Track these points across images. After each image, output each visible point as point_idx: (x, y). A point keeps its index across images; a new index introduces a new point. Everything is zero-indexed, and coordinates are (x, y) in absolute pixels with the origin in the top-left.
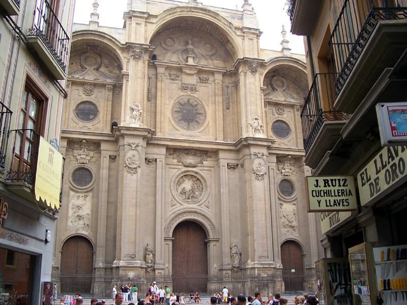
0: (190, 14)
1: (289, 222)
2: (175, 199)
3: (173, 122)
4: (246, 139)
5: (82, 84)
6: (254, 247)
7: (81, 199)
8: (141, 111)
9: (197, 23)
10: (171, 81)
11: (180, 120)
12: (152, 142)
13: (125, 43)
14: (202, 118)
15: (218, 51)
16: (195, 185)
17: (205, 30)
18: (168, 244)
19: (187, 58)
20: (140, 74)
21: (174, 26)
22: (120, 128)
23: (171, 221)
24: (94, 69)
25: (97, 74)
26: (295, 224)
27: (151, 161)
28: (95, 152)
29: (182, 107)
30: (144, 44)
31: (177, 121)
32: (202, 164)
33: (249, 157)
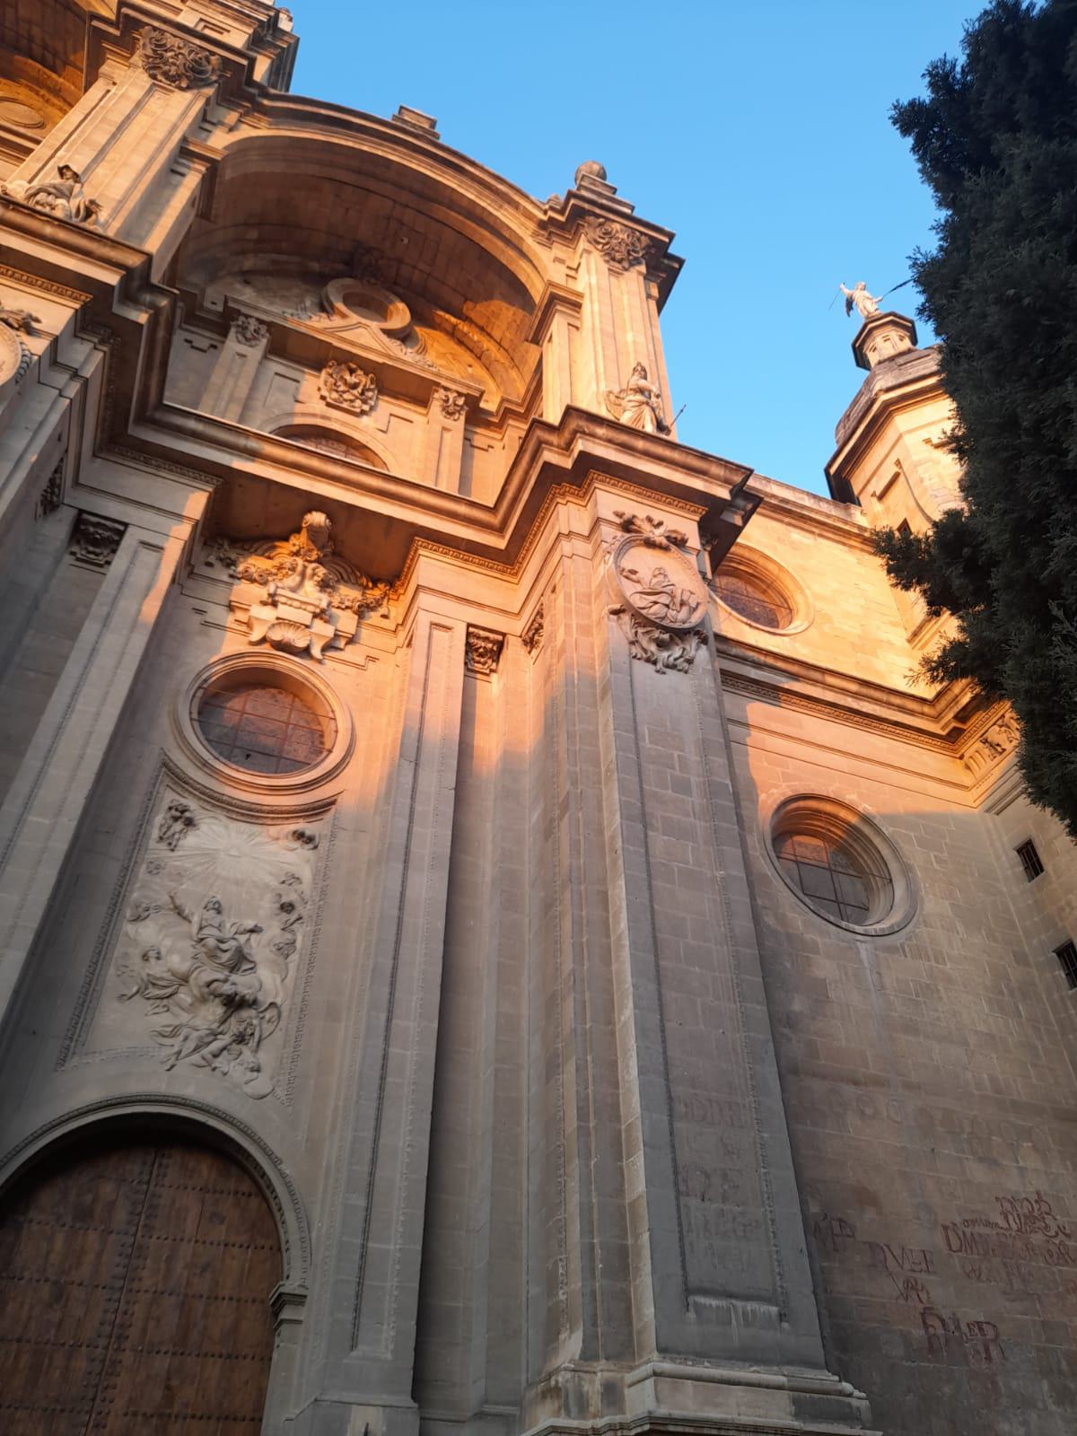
1: (212, 955)
26: (266, 980)
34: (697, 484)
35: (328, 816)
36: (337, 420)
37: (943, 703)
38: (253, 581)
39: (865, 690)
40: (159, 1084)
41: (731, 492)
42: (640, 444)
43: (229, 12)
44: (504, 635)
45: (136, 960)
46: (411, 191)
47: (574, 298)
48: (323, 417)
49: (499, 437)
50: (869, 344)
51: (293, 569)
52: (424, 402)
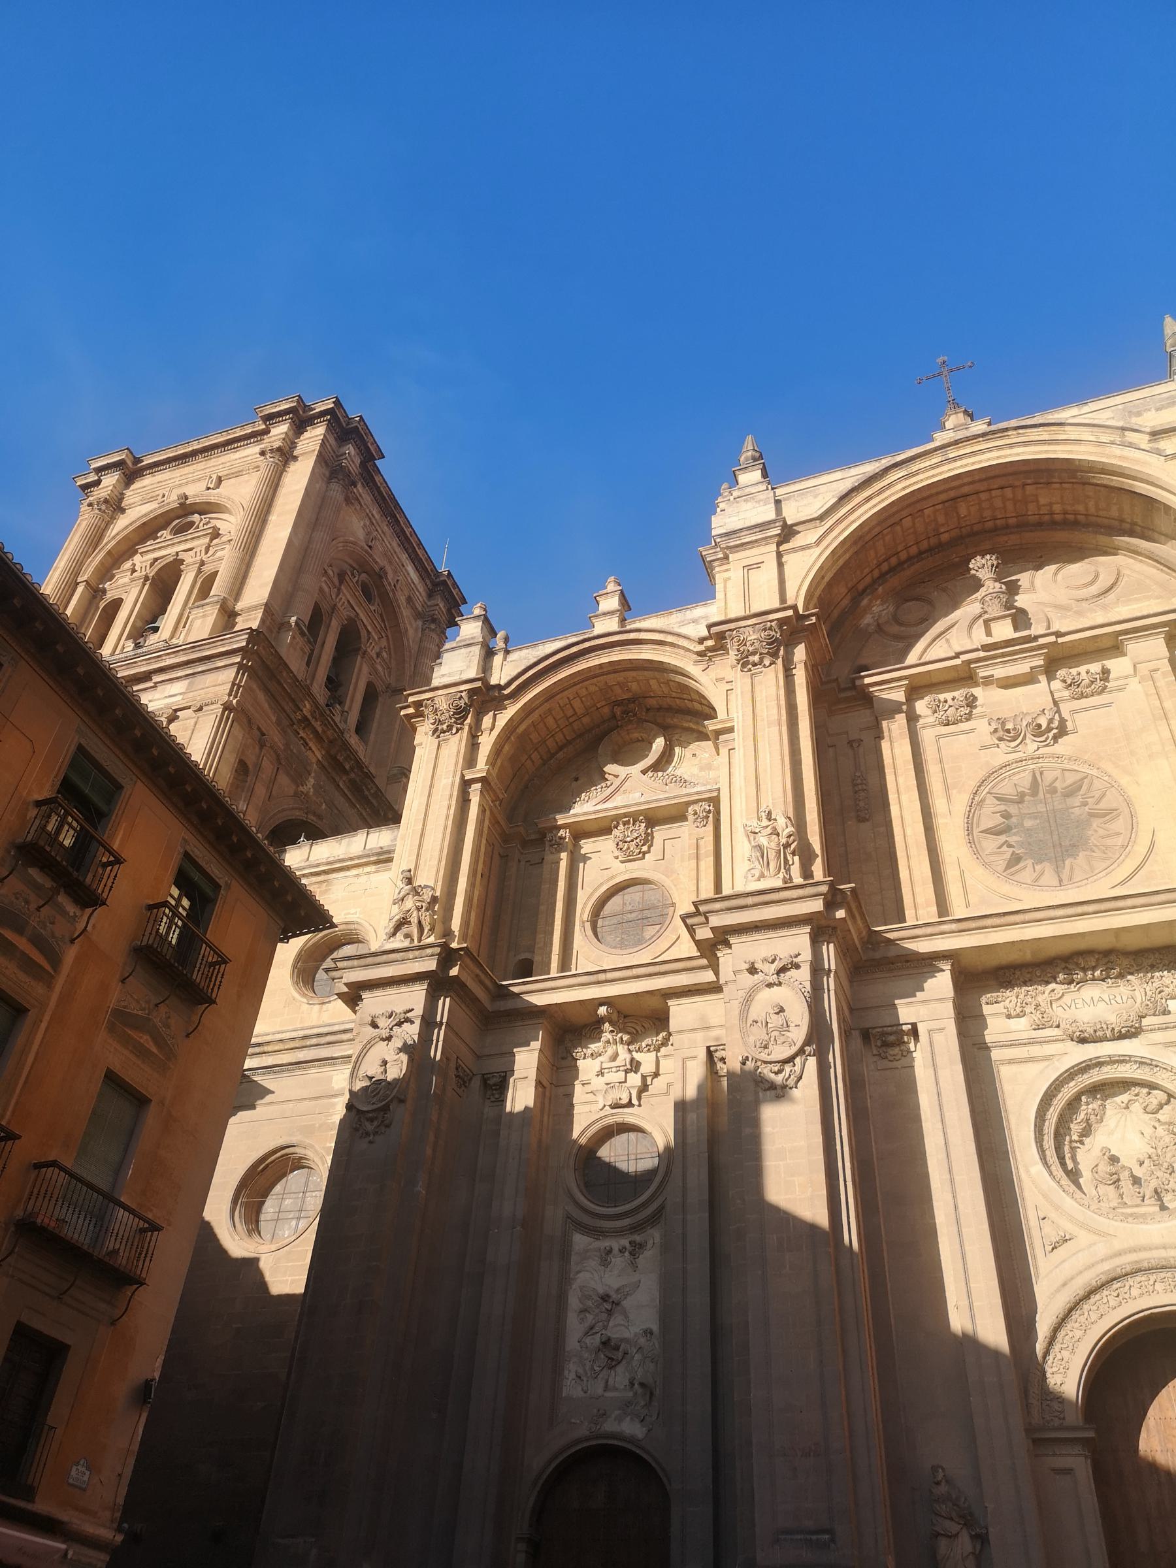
2: (1057, 1208)
3: (980, 871)
5: (603, 828)
7: (618, 1261)
8: (791, 829)
9: (998, 503)
11: (1015, 860)
12: (878, 955)
13: (705, 633)
14: (1119, 825)
15: (1127, 572)
16: (1161, 1131)
17: (1047, 518)
18: (1068, 1471)
19: (989, 633)
20: (775, 711)
21: (914, 550)
22: (702, 908)
23: (1056, 1329)
24: (644, 772)
25: (658, 784)
27: (892, 1038)
28: (663, 1050)
29: (1013, 809)
30: (777, 605)
31: (1000, 868)
32: (1166, 1012)
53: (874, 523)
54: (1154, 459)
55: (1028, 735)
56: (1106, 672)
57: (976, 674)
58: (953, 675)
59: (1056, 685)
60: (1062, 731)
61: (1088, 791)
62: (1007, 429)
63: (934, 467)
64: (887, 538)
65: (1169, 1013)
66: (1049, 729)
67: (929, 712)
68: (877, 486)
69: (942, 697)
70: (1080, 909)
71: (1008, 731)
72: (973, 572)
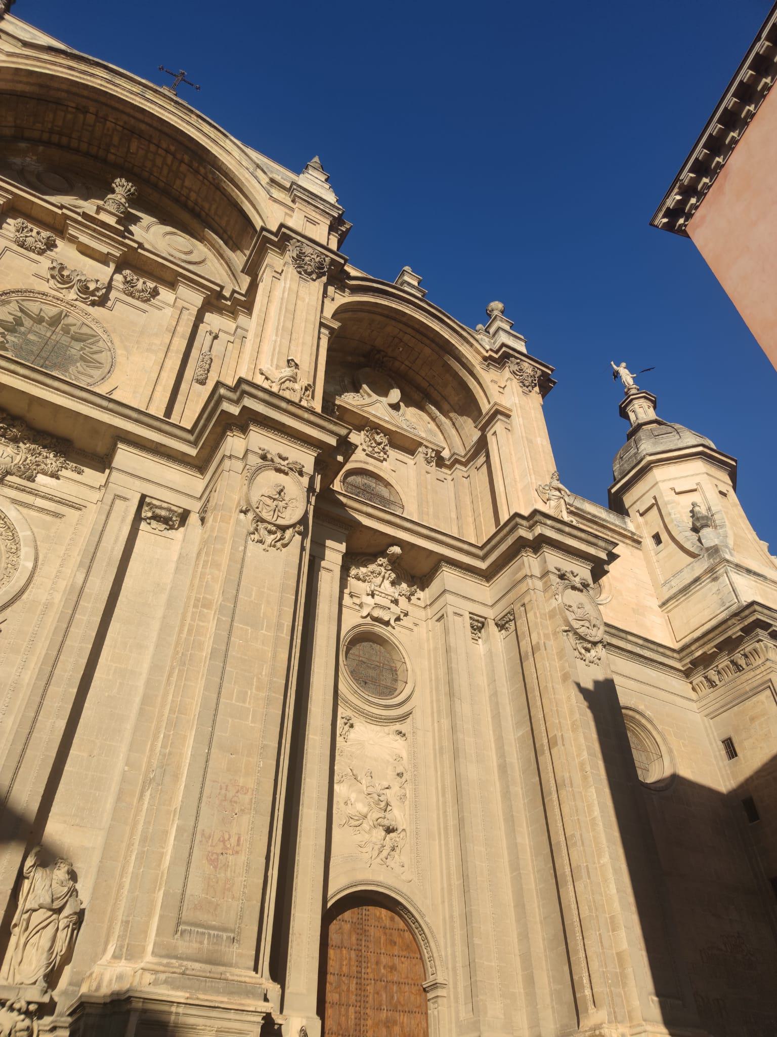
0: (138, 101)
4: (242, 387)
6: (162, 855)
9: (159, 162)
10: (15, 247)
14: (97, 374)
15: (210, 264)
17: (183, 198)
26: (398, 816)
29: (27, 322)
32: (31, 479)
33: (239, 465)
34: (592, 550)
35: (408, 720)
36: (372, 464)
37: (684, 653)
38: (359, 579)
39: (646, 644)
40: (367, 875)
41: (607, 555)
42: (567, 529)
43: (317, 210)
44: (486, 618)
45: (342, 804)
46: (413, 329)
47: (507, 412)
48: (365, 463)
49: (450, 472)
50: (629, 408)
51: (379, 574)
52: (412, 452)
53: (64, 87)
54: (263, 193)
55: (75, 287)
56: (155, 293)
57: (67, 229)
58: (49, 220)
59: (118, 278)
60: (102, 302)
61: (92, 344)
62: (192, 112)
63: (132, 92)
64: (69, 116)
65: (34, 481)
66: (93, 294)
67: (12, 229)
68: (83, 67)
69: (30, 226)
70: (13, 367)
71: (63, 276)
72: (114, 185)
